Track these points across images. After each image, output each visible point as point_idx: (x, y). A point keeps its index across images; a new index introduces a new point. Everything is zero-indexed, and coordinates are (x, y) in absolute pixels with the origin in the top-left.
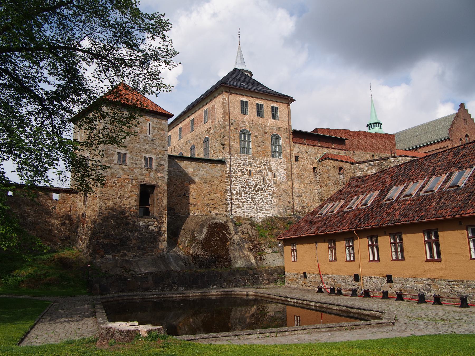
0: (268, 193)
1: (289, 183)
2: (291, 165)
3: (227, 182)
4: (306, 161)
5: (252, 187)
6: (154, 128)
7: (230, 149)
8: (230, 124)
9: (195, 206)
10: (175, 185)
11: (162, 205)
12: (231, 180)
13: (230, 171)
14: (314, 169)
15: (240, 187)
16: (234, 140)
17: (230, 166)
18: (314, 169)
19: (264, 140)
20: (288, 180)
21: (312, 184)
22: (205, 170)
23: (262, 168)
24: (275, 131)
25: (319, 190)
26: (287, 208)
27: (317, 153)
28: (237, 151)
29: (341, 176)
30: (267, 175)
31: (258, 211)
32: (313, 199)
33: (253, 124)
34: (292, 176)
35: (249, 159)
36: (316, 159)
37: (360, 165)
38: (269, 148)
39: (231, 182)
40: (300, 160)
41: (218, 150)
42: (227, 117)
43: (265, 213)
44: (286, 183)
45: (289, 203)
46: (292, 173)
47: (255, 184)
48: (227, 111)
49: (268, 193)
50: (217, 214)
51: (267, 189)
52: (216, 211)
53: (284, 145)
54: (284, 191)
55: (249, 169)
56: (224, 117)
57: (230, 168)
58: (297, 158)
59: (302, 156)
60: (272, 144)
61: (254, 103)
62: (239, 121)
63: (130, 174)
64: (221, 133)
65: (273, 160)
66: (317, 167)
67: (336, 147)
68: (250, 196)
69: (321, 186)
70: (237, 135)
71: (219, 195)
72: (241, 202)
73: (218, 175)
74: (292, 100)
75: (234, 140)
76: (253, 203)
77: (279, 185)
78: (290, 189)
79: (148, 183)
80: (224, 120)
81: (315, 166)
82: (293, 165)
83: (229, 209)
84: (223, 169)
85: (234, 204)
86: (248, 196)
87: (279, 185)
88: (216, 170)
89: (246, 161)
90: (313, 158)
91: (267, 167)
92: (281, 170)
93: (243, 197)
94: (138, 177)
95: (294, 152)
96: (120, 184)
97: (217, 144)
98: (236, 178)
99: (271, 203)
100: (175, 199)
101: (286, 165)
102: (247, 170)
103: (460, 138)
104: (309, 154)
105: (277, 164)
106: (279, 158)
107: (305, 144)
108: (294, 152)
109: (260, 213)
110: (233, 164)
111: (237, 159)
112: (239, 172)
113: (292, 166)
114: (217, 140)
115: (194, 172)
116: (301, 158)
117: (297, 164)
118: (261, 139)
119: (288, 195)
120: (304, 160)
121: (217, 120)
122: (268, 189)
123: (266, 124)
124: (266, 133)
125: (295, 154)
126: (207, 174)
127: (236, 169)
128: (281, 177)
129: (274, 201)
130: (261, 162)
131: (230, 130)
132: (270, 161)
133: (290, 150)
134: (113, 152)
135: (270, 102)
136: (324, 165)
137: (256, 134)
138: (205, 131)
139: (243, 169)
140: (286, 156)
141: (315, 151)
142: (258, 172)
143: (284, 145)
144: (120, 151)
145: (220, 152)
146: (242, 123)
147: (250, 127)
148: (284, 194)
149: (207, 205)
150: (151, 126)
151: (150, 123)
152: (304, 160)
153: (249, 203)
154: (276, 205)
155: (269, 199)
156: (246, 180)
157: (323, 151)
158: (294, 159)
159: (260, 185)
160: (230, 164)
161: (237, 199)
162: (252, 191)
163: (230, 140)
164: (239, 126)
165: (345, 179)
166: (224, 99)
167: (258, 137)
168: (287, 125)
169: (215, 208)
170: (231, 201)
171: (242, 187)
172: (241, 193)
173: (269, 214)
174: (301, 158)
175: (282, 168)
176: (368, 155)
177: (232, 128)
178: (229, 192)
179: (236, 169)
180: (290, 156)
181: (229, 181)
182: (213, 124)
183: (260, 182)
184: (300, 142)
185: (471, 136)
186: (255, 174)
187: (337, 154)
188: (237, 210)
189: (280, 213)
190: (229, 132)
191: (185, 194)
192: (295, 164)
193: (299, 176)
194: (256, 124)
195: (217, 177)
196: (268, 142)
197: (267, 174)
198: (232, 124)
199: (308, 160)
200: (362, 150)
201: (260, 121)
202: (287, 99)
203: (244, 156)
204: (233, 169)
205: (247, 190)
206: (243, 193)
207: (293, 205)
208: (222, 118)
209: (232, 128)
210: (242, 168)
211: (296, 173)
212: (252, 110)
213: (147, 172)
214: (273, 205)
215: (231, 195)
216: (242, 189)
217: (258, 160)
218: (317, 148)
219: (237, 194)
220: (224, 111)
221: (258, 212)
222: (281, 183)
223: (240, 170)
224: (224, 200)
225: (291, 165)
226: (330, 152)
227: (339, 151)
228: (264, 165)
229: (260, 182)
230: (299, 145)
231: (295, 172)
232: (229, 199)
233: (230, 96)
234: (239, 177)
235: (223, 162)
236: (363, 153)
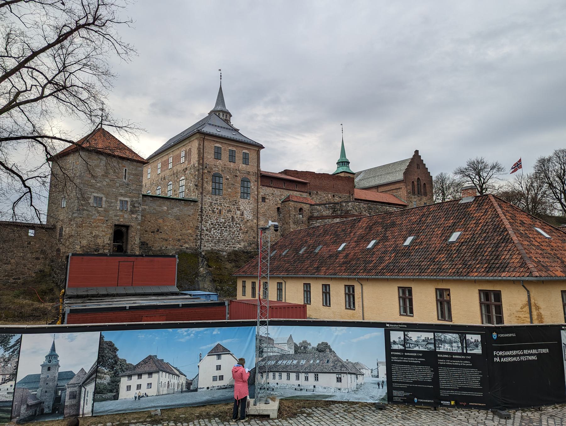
0: (235, 229)
1: (255, 221)
2: (258, 205)
3: (198, 219)
5: (221, 224)
6: (130, 174)
7: (202, 190)
8: (204, 167)
9: (167, 241)
10: (149, 221)
11: (134, 243)
12: (202, 218)
13: (202, 209)
14: (278, 208)
15: (209, 224)
16: (207, 182)
17: (202, 205)
18: (278, 208)
20: (254, 218)
22: (178, 208)
23: (232, 207)
24: (245, 175)
25: (281, 227)
26: (251, 243)
27: (282, 195)
28: (209, 191)
29: (301, 216)
30: (235, 214)
31: (226, 245)
32: (276, 235)
34: (258, 215)
35: (220, 199)
36: (280, 200)
37: (318, 207)
38: (239, 190)
39: (202, 220)
40: (267, 200)
41: (192, 190)
42: (201, 162)
43: (231, 247)
44: (252, 221)
45: (254, 238)
46: (258, 212)
47: (224, 221)
48: (202, 155)
49: (235, 229)
50: (187, 248)
51: (234, 226)
52: (187, 246)
53: (253, 187)
54: (250, 228)
55: (219, 208)
56: (199, 161)
57: (202, 207)
58: (264, 199)
59: (268, 197)
61: (227, 149)
62: (212, 165)
63: (105, 215)
64: (195, 175)
65: (242, 201)
66: (281, 207)
67: (299, 190)
68: (219, 232)
69: (283, 224)
70: (210, 178)
71: (190, 231)
72: (210, 237)
73: (190, 213)
74: (262, 147)
75: (207, 182)
76: (222, 239)
77: (246, 222)
78: (255, 225)
79: (122, 223)
80: (199, 164)
81: (279, 206)
82: (260, 205)
83: (199, 244)
84: (195, 208)
85: (203, 239)
86: (218, 232)
87: (246, 222)
88: (189, 210)
89: (217, 201)
90: (278, 199)
91: (236, 206)
92: (248, 210)
93: (213, 233)
94: (113, 218)
95: (261, 194)
96: (95, 224)
97: (191, 185)
98: (207, 216)
99: (238, 238)
100: (149, 234)
102: (217, 209)
103: (412, 181)
105: (245, 204)
106: (247, 199)
107: (271, 187)
108: (262, 194)
109: (227, 247)
110: (205, 204)
111: (209, 199)
112: (210, 210)
113: (259, 206)
114: (192, 181)
115: (167, 210)
116: (267, 199)
119: (254, 232)
121: (192, 163)
122: (236, 226)
123: (237, 168)
124: (236, 176)
125: (262, 195)
126: (180, 212)
127: (208, 208)
128: (248, 216)
129: (240, 236)
130: (231, 202)
131: (203, 172)
132: (239, 202)
133: (258, 192)
134: (90, 196)
135: (242, 149)
136: (286, 206)
137: (228, 177)
138: (181, 171)
139: (214, 208)
140: (253, 197)
141: (279, 193)
142: (228, 211)
143: (253, 187)
144: (96, 195)
145: (194, 192)
146: (214, 167)
147: (222, 171)
148: (250, 230)
149: (179, 240)
150: (127, 171)
151: (126, 169)
153: (217, 238)
154: (242, 240)
155: (236, 234)
156: (216, 218)
157: (286, 193)
158: (260, 200)
159: (228, 223)
160: (202, 204)
161: (207, 234)
162: (221, 228)
163: (203, 182)
164: (212, 169)
165: (304, 219)
166: (199, 145)
167: (229, 180)
168: (257, 169)
169: (185, 243)
170: (201, 236)
171: (212, 224)
172: (211, 229)
173: (236, 248)
174: (267, 199)
175: (249, 208)
176: (330, 195)
177: (206, 171)
178: (199, 228)
179: (208, 208)
180: (258, 197)
181: (200, 218)
182: (189, 166)
183: (229, 220)
184: (268, 185)
185: (422, 179)
186: (225, 213)
187: (299, 196)
188: (206, 245)
189: (245, 247)
190: (202, 175)
191: (158, 230)
193: (264, 215)
195: (189, 215)
196: (238, 185)
197: (236, 212)
198: (206, 167)
199: (273, 201)
200: (325, 190)
201: (232, 165)
202: (258, 146)
203: (215, 197)
204: (205, 208)
205: (216, 227)
206: (213, 229)
207: (257, 240)
208: (197, 161)
209: (206, 171)
210: (213, 207)
211: (262, 212)
212: (225, 156)
213: (121, 213)
214: (240, 240)
215: (201, 231)
216: (212, 226)
217: (228, 201)
218: (282, 190)
219: (207, 230)
220: (199, 155)
221: (225, 246)
222: (248, 221)
223: (211, 209)
224: (195, 236)
225: (258, 205)
227: (301, 193)
228: (234, 205)
229: (229, 220)
230: (266, 187)
231: (261, 211)
232: (199, 235)
233: (206, 143)
234: (210, 215)
235: (195, 201)
236: (325, 193)
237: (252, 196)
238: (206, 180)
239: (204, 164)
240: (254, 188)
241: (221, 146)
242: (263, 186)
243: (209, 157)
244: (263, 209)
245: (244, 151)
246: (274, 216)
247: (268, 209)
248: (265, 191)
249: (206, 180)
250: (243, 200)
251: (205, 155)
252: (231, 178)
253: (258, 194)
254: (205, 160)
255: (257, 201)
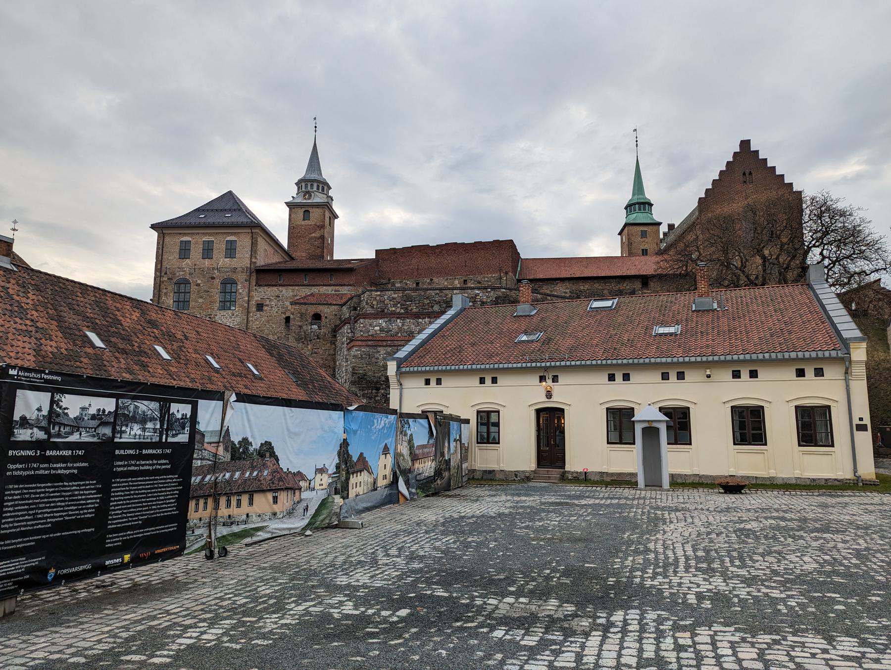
2: (247, 318)
4: (275, 310)
16: (166, 293)
19: (210, 288)
21: (280, 340)
24: (227, 274)
33: (194, 269)
38: (217, 298)
40: (265, 308)
42: (159, 267)
58: (260, 307)
59: (268, 303)
60: (224, 292)
61: (200, 240)
82: (252, 317)
95: (256, 299)
101: (240, 317)
104: (281, 298)
105: (226, 318)
106: (230, 309)
113: (251, 319)
116: (266, 305)
117: (258, 315)
118: (205, 288)
120: (272, 307)
123: (215, 266)
124: (213, 278)
132: (216, 315)
133: (249, 297)
137: (199, 282)
140: (241, 306)
147: (190, 274)
152: (272, 307)
158: (254, 309)
164: (175, 274)
167: (201, 285)
168: (249, 262)
174: (267, 305)
175: (233, 323)
177: (165, 279)
180: (248, 305)
187: (333, 292)
190: (160, 285)
192: (255, 316)
194: (200, 269)
198: (166, 273)
201: (207, 263)
209: (165, 279)
211: (255, 327)
212: (196, 252)
218: (297, 288)
225: (247, 318)
226: (319, 291)
230: (265, 288)
237: (238, 304)
238: (165, 291)
239: (163, 268)
240: (243, 291)
241: (191, 239)
242: (260, 286)
243: (172, 258)
244: (258, 323)
245: (229, 238)
246: (278, 332)
247: (268, 322)
248: (262, 293)
249: (165, 291)
250: (223, 313)
251: (164, 257)
252: (205, 282)
253: (249, 301)
254: (164, 264)
255: (246, 311)
